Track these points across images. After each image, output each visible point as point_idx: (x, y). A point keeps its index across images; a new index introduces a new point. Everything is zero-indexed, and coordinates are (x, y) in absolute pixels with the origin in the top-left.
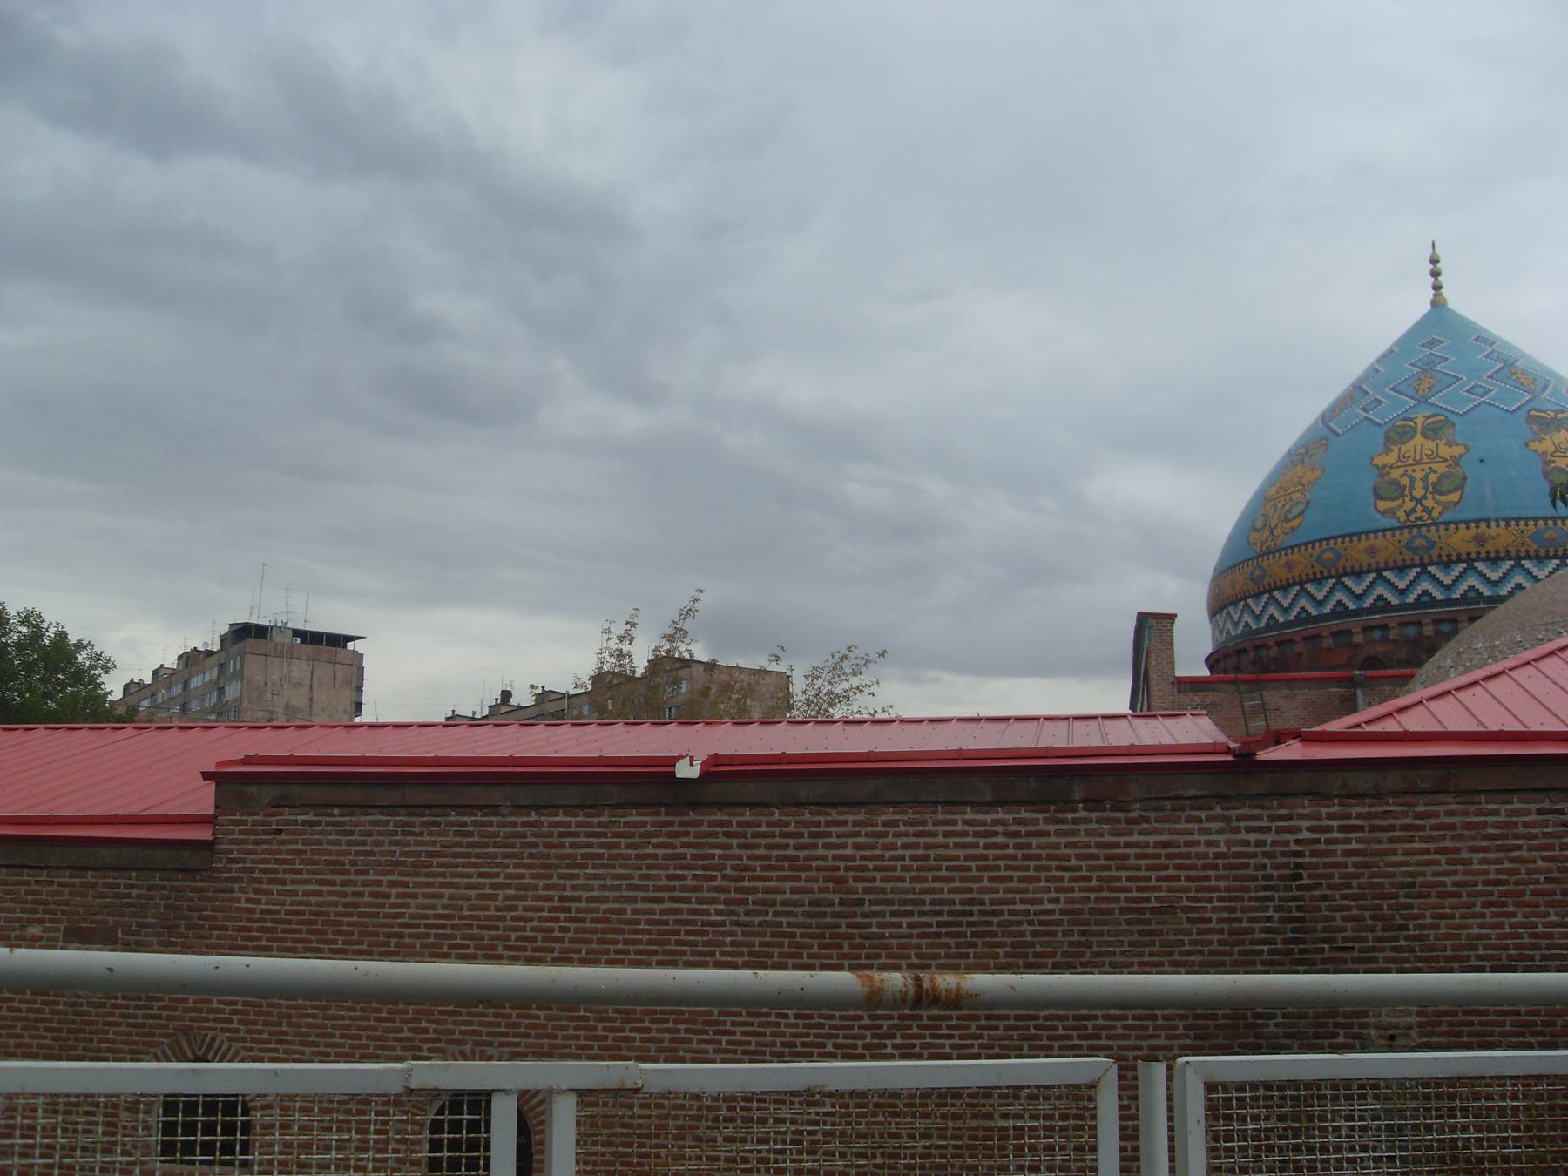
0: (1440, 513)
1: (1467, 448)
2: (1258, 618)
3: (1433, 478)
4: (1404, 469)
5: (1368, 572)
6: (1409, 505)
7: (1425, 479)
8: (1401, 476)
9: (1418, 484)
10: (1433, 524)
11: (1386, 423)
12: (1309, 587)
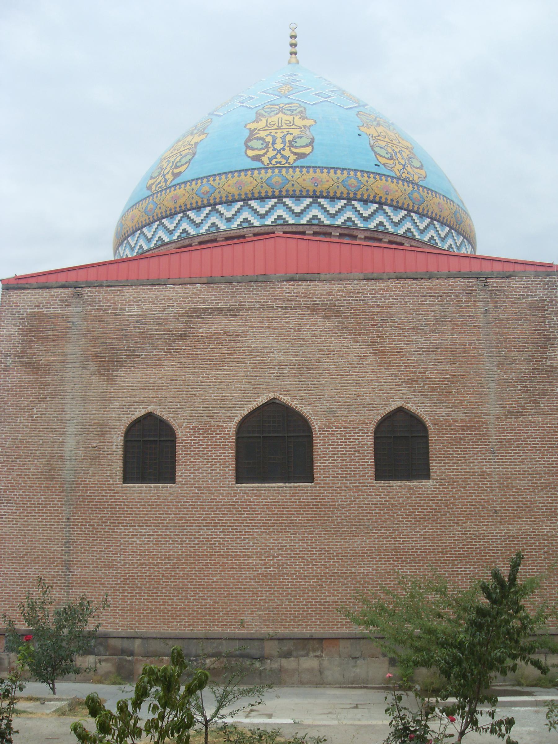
0: (295, 161)
1: (315, 121)
2: (149, 240)
3: (289, 138)
4: (270, 131)
5: (239, 201)
6: (271, 153)
7: (284, 136)
8: (267, 136)
9: (279, 141)
10: (291, 167)
11: (256, 107)
12: (190, 214)
